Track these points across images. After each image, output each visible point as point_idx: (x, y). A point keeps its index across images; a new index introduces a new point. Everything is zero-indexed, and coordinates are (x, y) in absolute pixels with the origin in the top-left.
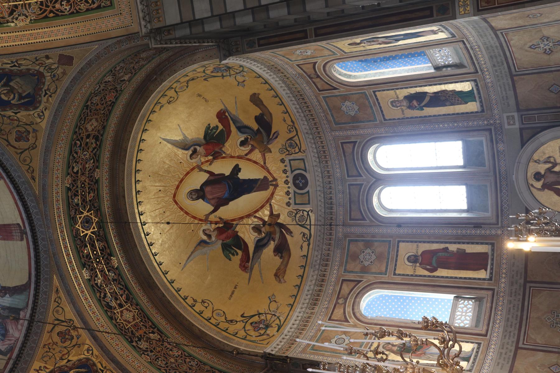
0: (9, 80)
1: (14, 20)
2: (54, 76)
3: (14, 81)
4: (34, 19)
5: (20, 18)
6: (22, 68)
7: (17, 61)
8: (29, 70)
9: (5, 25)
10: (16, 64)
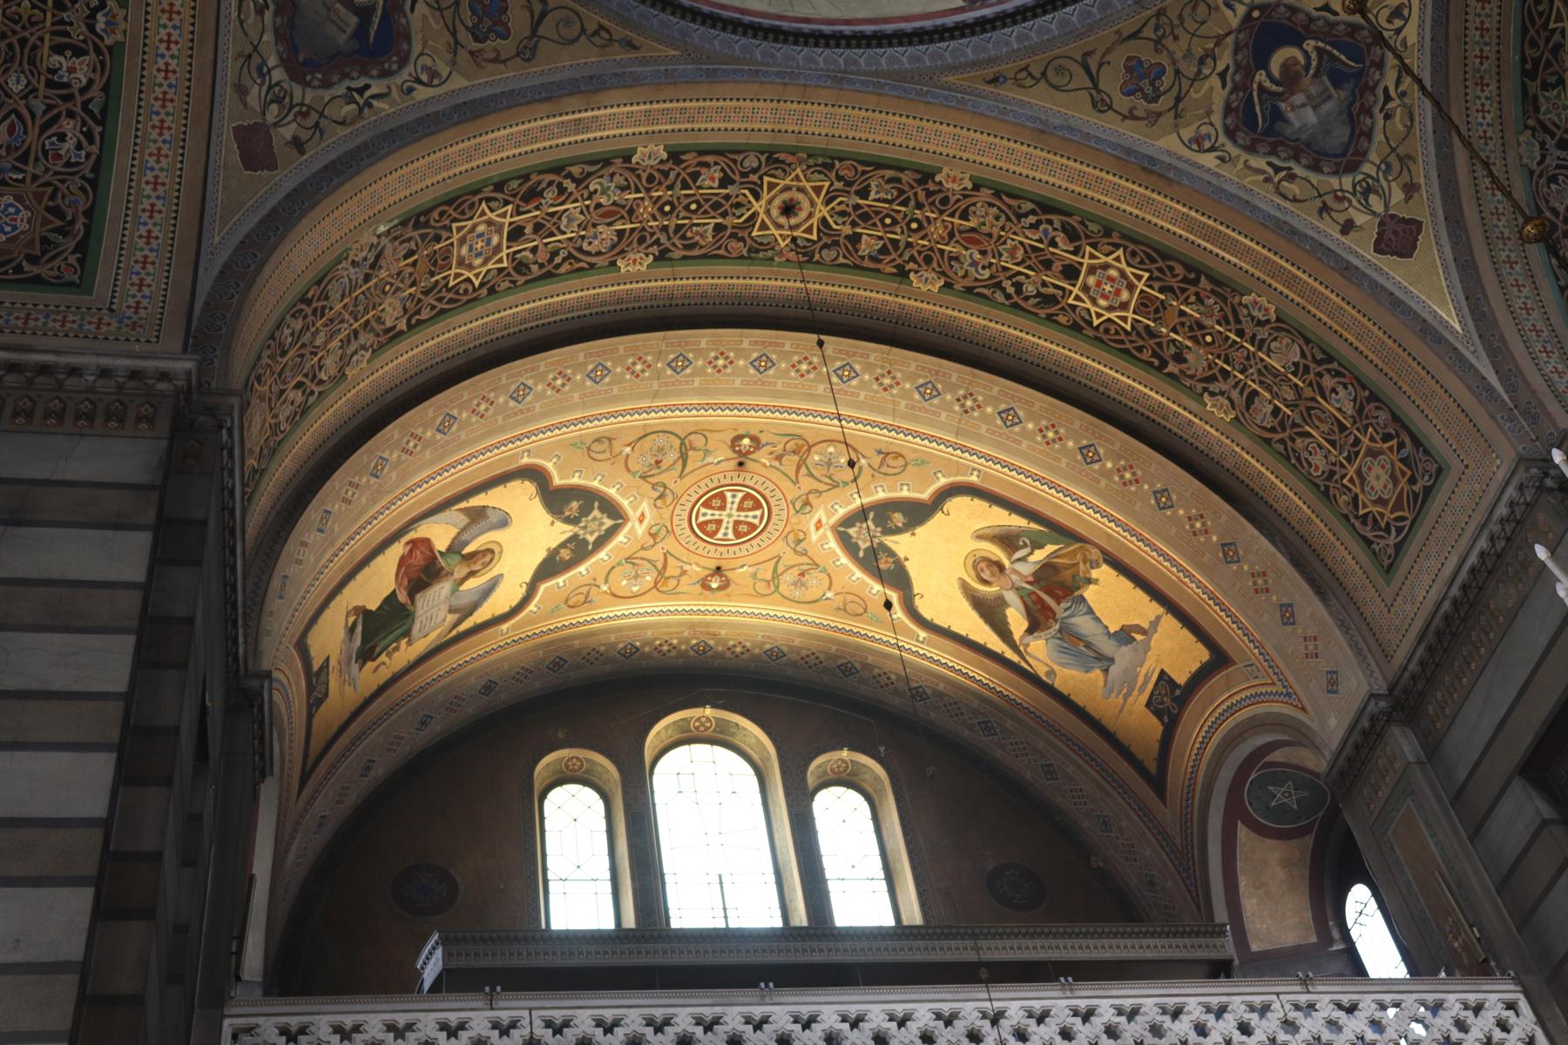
0: (361, 32)
1: (375, 240)
2: (262, 75)
3: (349, 30)
4: (341, 262)
5: (364, 254)
6: (340, 90)
7: (361, 110)
8: (327, 84)
9: (396, 222)
10: (361, 102)
